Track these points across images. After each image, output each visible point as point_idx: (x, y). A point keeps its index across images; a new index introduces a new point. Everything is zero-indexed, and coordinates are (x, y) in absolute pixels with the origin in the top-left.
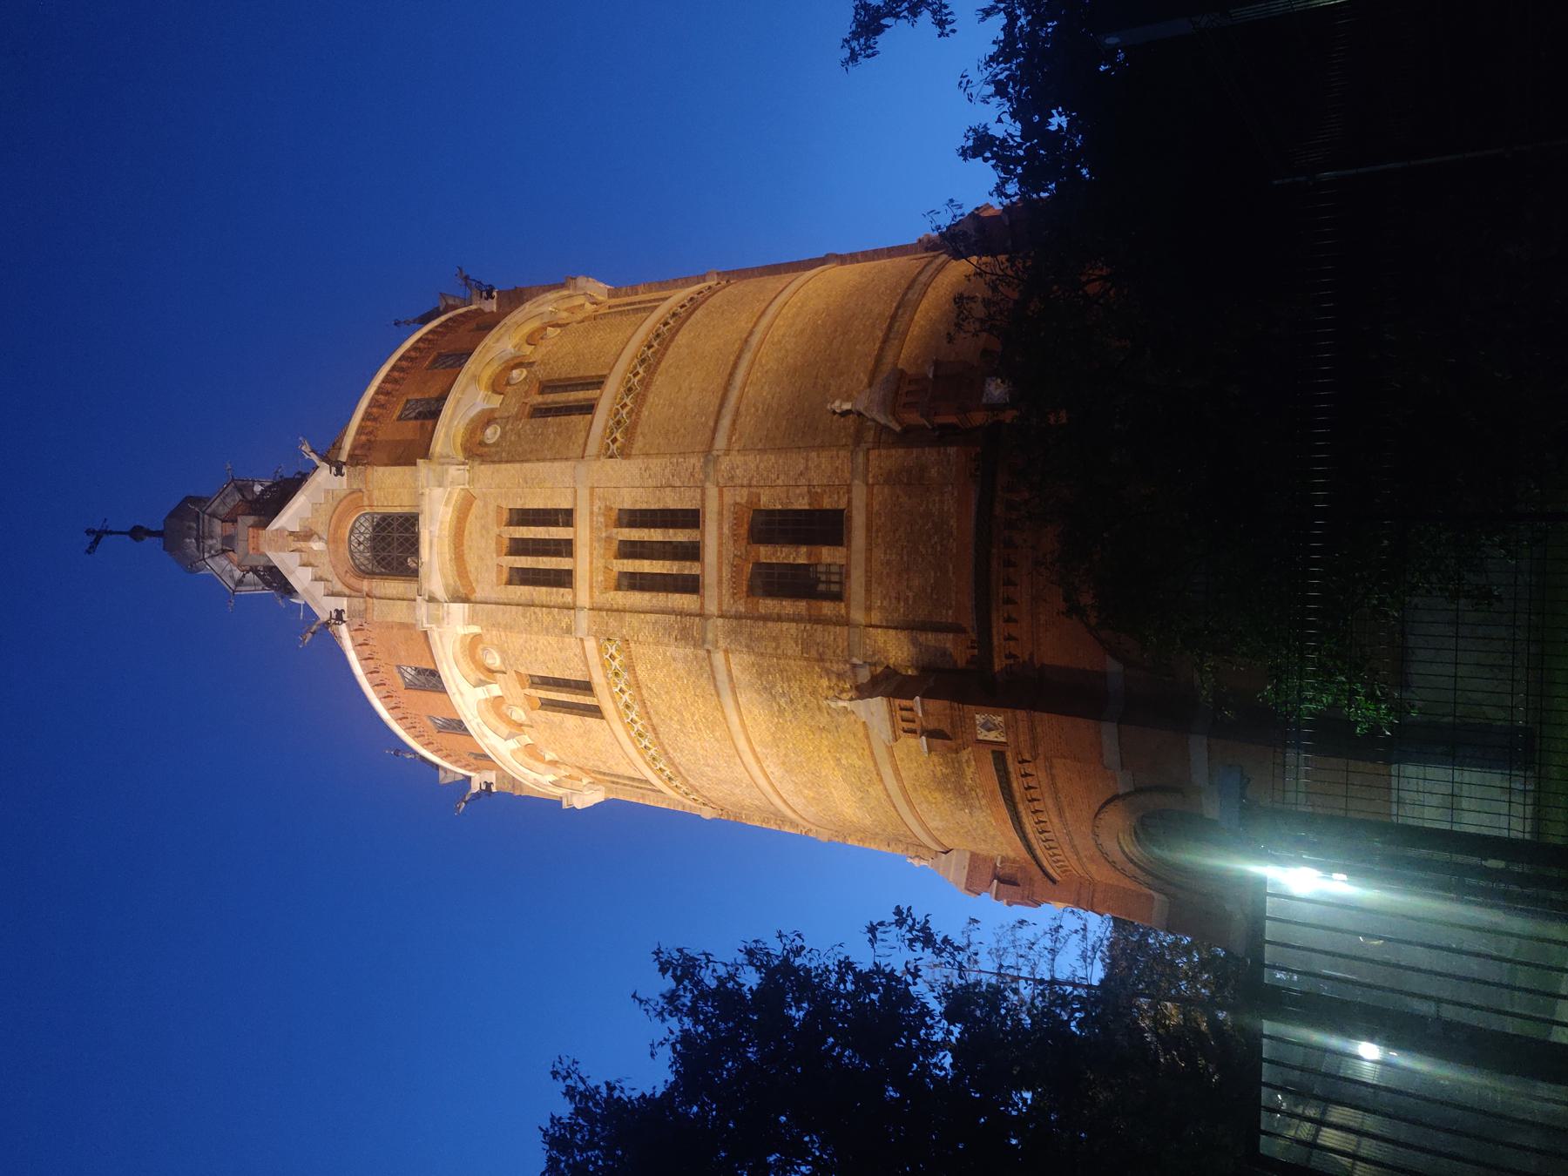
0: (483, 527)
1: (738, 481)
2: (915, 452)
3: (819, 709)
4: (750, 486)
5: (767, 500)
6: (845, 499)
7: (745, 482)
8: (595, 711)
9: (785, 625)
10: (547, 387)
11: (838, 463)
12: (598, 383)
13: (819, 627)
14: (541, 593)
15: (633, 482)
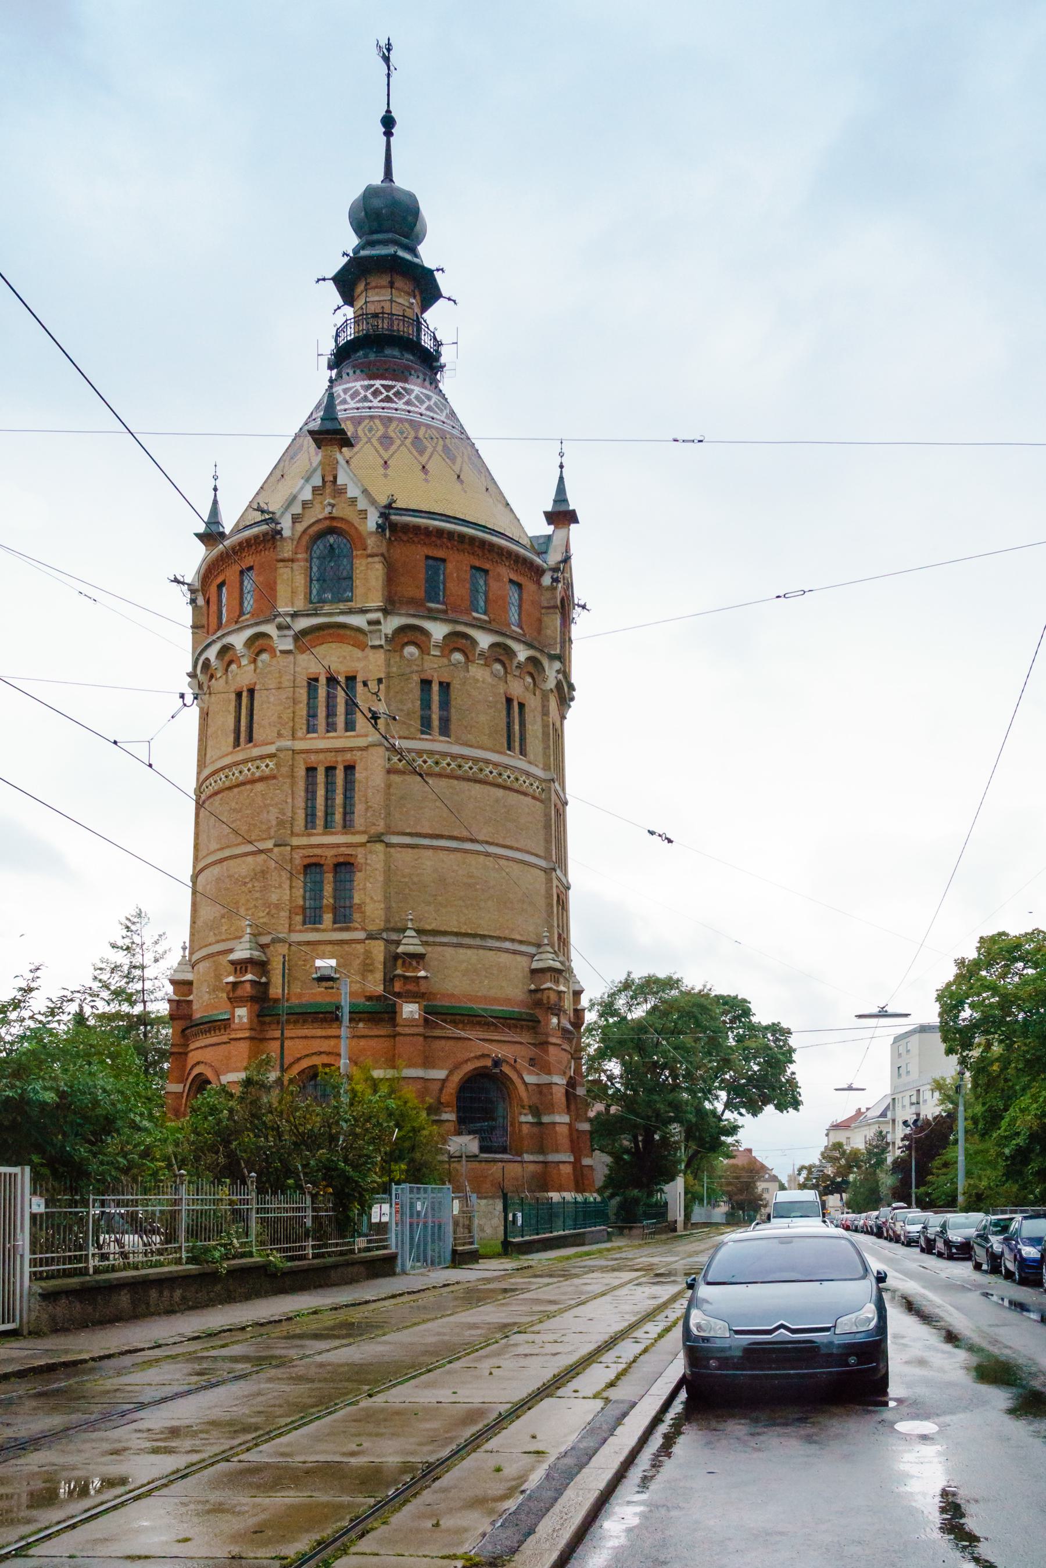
0: (345, 658)
1: (369, 857)
2: (381, 967)
3: (247, 910)
4: (366, 864)
5: (358, 874)
6: (357, 925)
7: (369, 861)
8: (237, 743)
9: (288, 892)
10: (445, 687)
11: (377, 921)
12: (445, 729)
13: (287, 914)
14: (302, 710)
15: (372, 773)
